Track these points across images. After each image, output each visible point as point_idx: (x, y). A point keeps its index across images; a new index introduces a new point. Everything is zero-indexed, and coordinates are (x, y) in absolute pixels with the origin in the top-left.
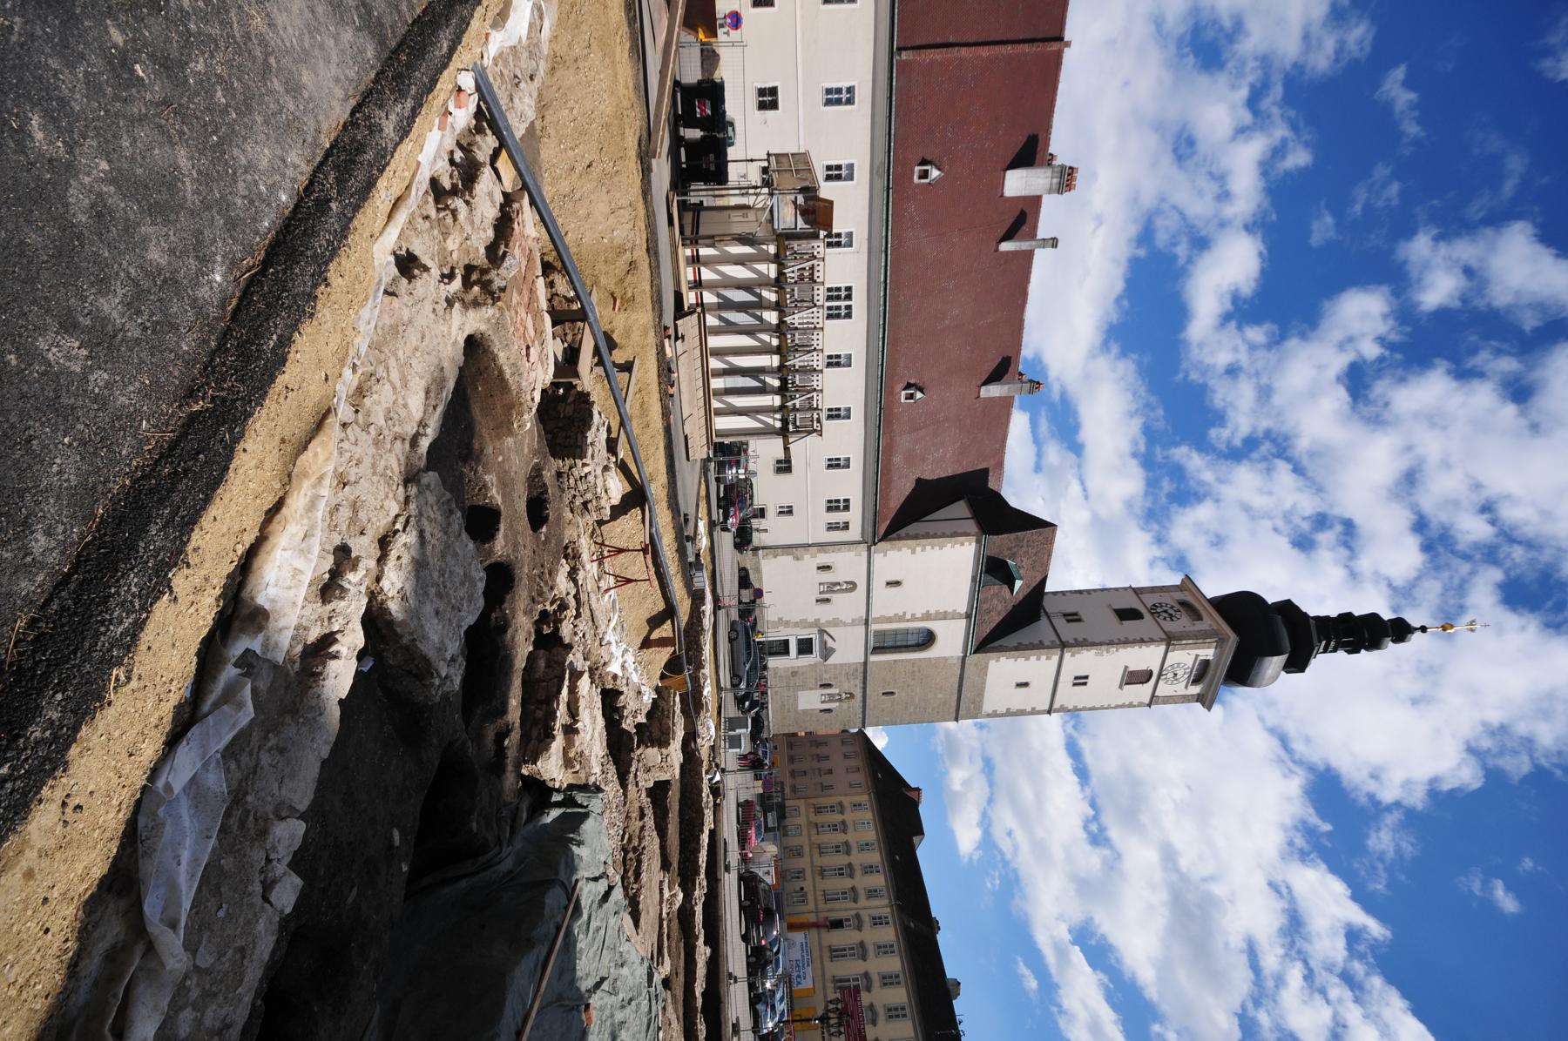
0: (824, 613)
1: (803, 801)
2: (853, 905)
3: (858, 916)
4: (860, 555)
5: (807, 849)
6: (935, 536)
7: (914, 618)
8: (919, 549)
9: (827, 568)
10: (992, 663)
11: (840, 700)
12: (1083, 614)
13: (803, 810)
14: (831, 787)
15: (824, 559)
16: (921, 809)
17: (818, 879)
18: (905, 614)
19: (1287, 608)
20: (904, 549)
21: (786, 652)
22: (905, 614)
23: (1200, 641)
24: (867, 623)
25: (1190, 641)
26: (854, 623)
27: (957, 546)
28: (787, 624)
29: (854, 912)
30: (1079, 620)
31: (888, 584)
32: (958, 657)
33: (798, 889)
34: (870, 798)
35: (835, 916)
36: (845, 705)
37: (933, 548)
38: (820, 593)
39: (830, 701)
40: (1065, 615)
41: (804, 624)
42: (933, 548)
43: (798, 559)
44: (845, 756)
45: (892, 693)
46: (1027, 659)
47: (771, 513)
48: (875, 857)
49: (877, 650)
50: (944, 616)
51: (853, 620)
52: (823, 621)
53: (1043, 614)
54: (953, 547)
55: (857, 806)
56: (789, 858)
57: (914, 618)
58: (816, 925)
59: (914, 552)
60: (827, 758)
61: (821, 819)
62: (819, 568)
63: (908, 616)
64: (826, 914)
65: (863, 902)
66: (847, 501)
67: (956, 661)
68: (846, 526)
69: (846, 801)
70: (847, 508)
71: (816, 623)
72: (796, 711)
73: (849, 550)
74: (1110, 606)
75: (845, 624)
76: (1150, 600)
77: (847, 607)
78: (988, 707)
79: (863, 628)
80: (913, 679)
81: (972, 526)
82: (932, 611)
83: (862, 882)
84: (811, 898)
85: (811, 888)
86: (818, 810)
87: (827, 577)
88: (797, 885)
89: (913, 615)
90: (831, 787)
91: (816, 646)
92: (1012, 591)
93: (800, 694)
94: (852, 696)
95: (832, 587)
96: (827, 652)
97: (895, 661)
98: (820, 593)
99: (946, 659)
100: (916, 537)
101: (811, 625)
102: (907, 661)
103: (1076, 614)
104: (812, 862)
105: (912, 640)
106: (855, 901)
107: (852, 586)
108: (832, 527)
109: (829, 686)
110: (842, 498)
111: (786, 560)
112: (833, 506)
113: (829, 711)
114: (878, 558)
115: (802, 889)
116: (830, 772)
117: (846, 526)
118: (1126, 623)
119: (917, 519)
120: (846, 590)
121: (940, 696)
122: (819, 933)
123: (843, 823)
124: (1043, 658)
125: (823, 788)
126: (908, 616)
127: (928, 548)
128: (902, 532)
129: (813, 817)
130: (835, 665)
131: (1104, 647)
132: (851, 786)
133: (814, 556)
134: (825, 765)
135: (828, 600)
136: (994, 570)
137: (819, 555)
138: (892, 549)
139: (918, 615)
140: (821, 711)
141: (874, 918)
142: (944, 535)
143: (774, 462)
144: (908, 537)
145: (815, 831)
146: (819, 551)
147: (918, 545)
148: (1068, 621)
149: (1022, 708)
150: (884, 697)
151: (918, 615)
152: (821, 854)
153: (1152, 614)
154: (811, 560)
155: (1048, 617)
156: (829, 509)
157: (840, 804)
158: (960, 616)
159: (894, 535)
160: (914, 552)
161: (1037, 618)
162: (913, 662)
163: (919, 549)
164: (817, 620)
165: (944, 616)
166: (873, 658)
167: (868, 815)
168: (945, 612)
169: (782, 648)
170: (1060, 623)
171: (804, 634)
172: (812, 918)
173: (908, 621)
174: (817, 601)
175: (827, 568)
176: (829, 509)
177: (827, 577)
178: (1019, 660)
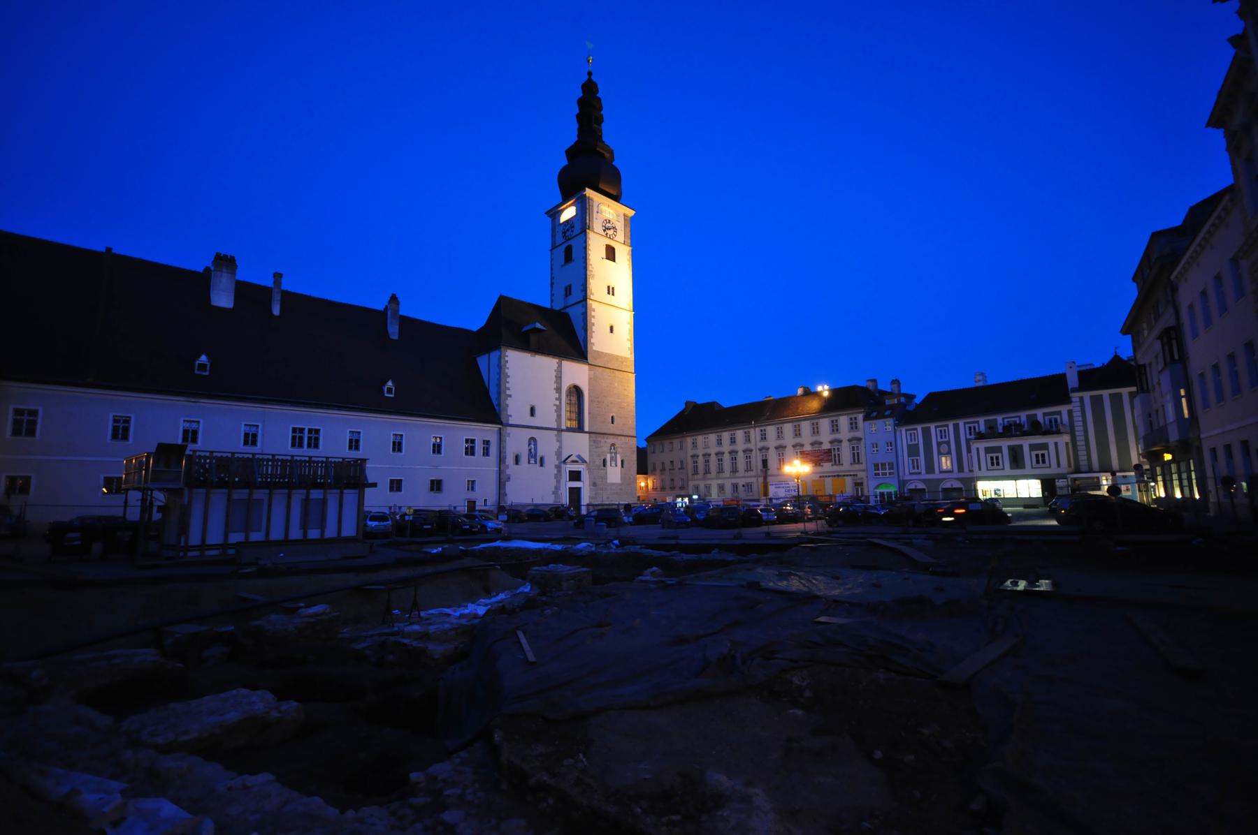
0: (551, 461)
1: (690, 483)
2: (754, 452)
3: (760, 450)
4: (509, 434)
5: (720, 481)
6: (499, 380)
7: (559, 399)
8: (508, 392)
9: (517, 460)
10: (594, 348)
11: (616, 453)
12: (567, 284)
13: (696, 483)
14: (682, 462)
15: (510, 460)
16: (700, 402)
17: (737, 474)
18: (555, 405)
19: (570, 153)
20: (507, 402)
21: (579, 489)
22: (555, 405)
23: (588, 211)
25: (588, 217)
26: (559, 440)
28: (557, 488)
29: (758, 452)
30: (570, 286)
32: (590, 370)
33: (743, 488)
34: (689, 436)
35: (760, 464)
36: (619, 450)
38: (536, 462)
39: (616, 461)
40: (566, 296)
41: (558, 476)
43: (509, 478)
44: (663, 451)
46: (593, 324)
47: (472, 496)
48: (726, 436)
51: (558, 441)
52: (557, 463)
53: (562, 311)
55: (695, 445)
56: (724, 493)
57: (559, 399)
58: (765, 478)
59: (510, 396)
60: (663, 463)
61: (701, 470)
63: (557, 403)
64: (759, 471)
65: (751, 446)
66: (467, 441)
67: (592, 372)
69: (691, 452)
70: (473, 441)
71: (558, 467)
72: (621, 484)
73: (505, 441)
74: (562, 266)
75: (560, 447)
76: (560, 239)
77: (547, 444)
79: (563, 433)
81: (494, 355)
82: (555, 386)
83: (740, 445)
84: (749, 480)
85: (743, 479)
86: (696, 472)
87: (524, 459)
88: (741, 489)
89: (557, 399)
90: (682, 462)
91: (575, 467)
92: (543, 330)
94: (613, 445)
95: (532, 455)
96: (581, 460)
97: (589, 413)
99: (590, 379)
100: (499, 393)
101: (559, 471)
103: (566, 288)
104: (729, 478)
105: (574, 399)
106: (751, 450)
107: (533, 440)
108: (486, 453)
109: (604, 461)
110: (465, 445)
111: (509, 487)
112: (470, 451)
113: (622, 461)
114: (511, 421)
115: (743, 486)
116: (672, 462)
117: (487, 443)
118: (573, 257)
119: (486, 392)
120: (535, 445)
122: (771, 476)
123: (704, 455)
124: (593, 314)
125: (682, 468)
126: (557, 403)
127: (507, 385)
128: (495, 402)
129: (700, 476)
130: (590, 456)
131: (588, 272)
132: (681, 448)
133: (508, 467)
134: (668, 466)
135: (542, 459)
136: (527, 343)
137: (507, 464)
138: (507, 411)
139: (557, 395)
140: (622, 467)
141: (762, 439)
142: (499, 373)
143: (432, 493)
144: (499, 399)
145: (709, 475)
146: (505, 463)
147: (505, 392)
148: (570, 294)
151: (557, 395)
152: (723, 472)
153: (569, 239)
154: (511, 469)
155: (567, 307)
156: (473, 454)
157: (692, 456)
158: (560, 366)
159: (496, 408)
160: (510, 396)
161: (567, 315)
162: (591, 402)
163: (508, 392)
164: (556, 467)
165: (559, 378)
166: (586, 429)
167: (700, 439)
168: (556, 377)
169: (575, 493)
170: (571, 300)
171: (566, 476)
172: (761, 480)
173: (560, 403)
175: (517, 460)
176: (473, 454)
177: (524, 459)
178: (593, 330)
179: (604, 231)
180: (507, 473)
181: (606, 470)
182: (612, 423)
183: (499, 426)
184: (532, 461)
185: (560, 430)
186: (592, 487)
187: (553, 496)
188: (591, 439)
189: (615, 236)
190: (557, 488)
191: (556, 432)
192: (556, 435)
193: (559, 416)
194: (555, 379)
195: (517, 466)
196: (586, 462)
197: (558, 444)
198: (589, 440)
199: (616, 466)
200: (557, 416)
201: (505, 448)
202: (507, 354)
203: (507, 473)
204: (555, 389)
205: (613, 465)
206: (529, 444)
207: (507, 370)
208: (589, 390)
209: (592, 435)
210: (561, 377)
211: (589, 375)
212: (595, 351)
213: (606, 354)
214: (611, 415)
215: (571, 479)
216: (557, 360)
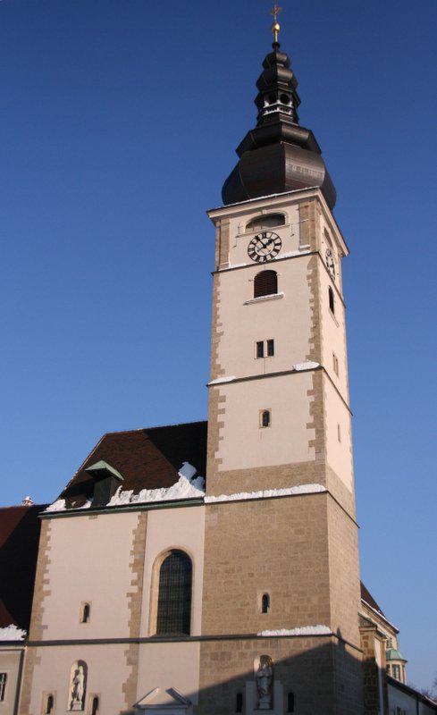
7: (139, 582)
8: (46, 587)
18: (128, 595)
20: (43, 605)
22: (128, 595)
24: (136, 641)
26: (133, 662)
27: (49, 544)
31: (85, 621)
37: (47, 571)
42: (47, 571)
49: (186, 629)
51: (130, 662)
54: (49, 549)
59: (48, 593)
63: (135, 589)
67: (215, 516)
78: (311, 455)
79: (142, 646)
80: (240, 570)
82: (131, 560)
89: (134, 583)
97: (205, 598)
99: (209, 530)
102: (206, 579)
114: (46, 637)
126: (135, 589)
127: (46, 577)
139: (135, 576)
151: (135, 576)
160: (48, 593)
162: (209, 574)
166: (197, 629)
168: (135, 542)
173: (141, 589)
178: (221, 435)
179: (251, 256)
182: (265, 611)
185: (136, 641)
188: (208, 651)
189: (277, 251)
191: (126, 646)
192: (127, 652)
197: (131, 667)
200: (133, 613)
202: (50, 526)
204: (130, 565)
207: (47, 553)
208: (206, 551)
212: (222, 474)
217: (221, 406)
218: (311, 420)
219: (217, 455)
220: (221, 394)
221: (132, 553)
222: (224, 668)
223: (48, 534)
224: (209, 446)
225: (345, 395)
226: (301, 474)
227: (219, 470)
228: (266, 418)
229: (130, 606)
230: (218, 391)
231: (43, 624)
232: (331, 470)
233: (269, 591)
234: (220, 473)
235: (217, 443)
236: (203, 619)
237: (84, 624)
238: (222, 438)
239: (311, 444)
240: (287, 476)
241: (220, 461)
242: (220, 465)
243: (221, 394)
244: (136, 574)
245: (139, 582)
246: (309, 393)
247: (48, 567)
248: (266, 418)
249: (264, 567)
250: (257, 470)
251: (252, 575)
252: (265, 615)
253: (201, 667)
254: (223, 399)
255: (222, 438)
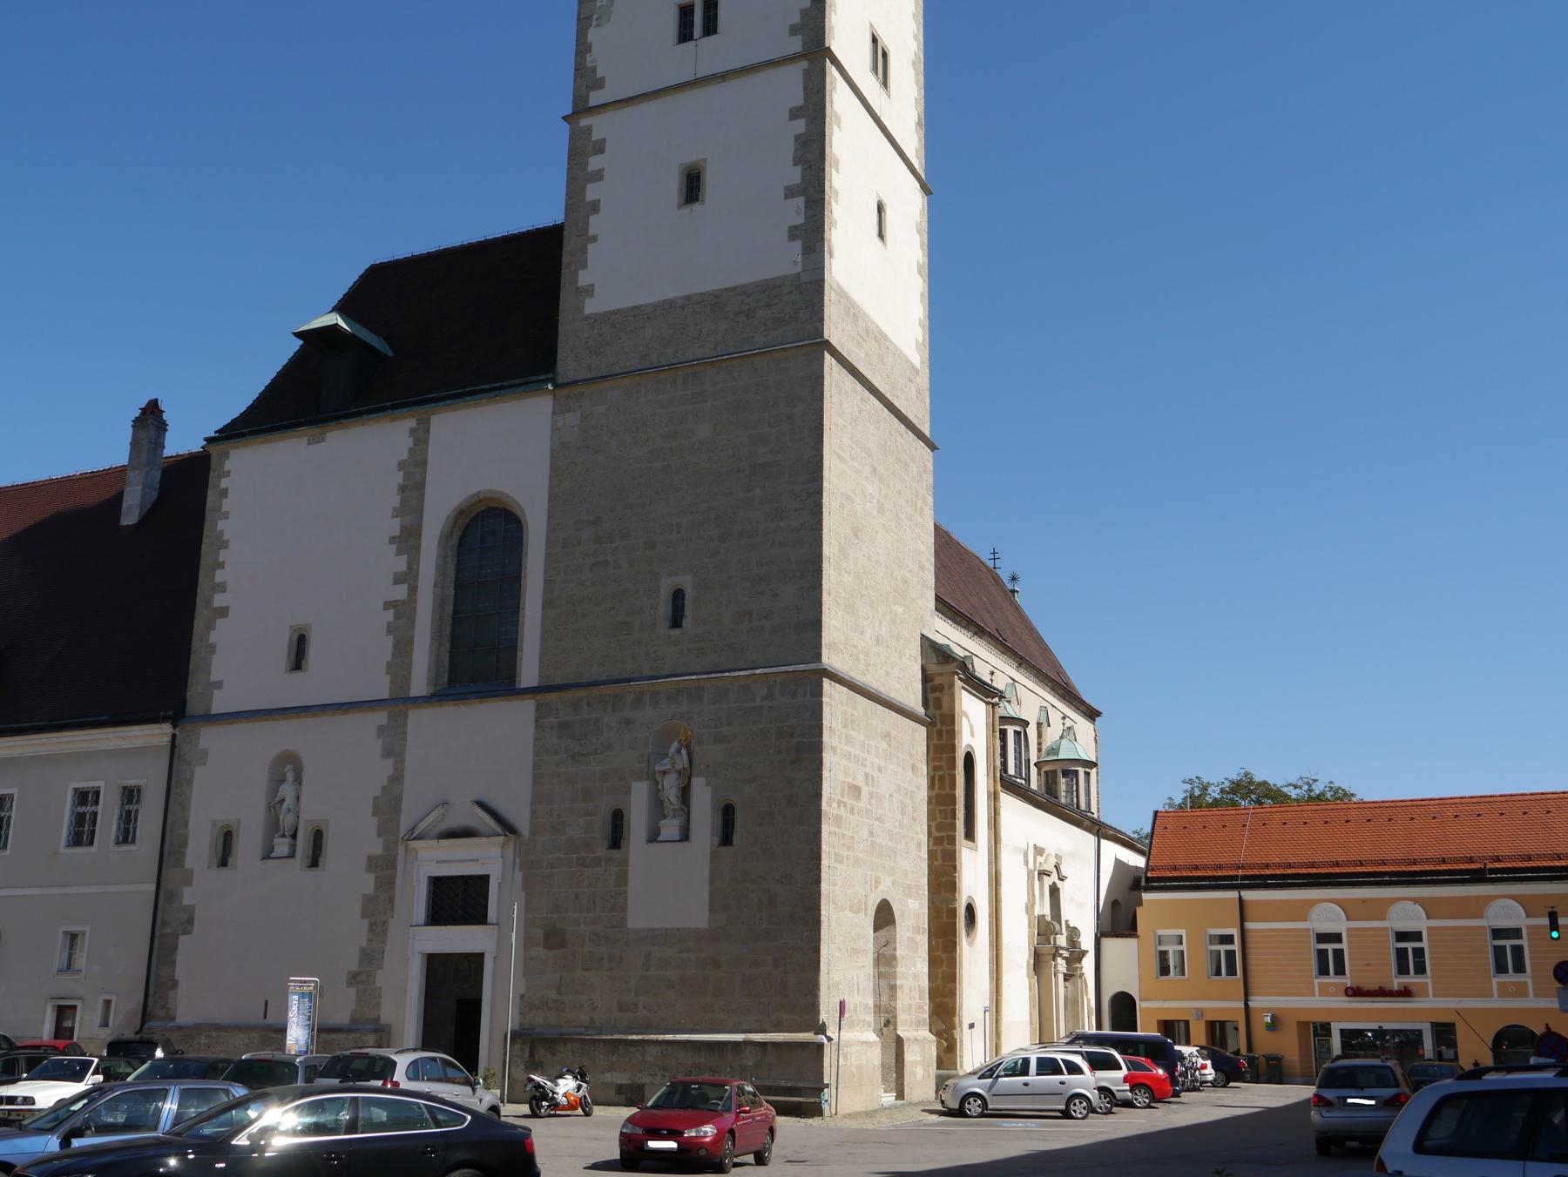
4: (205, 752)
7: (408, 578)
18: (388, 605)
20: (214, 637)
21: (473, 962)
22: (388, 605)
26: (394, 749)
27: (227, 505)
37: (221, 565)
38: (292, 855)
41: (378, 909)
42: (221, 565)
43: (190, 921)
45: (678, 596)
50: (413, 488)
51: (388, 752)
52: (376, 847)
59: (223, 612)
62: (224, 863)
63: (401, 592)
67: (573, 418)
68: (131, 795)
71: (384, 868)
73: (190, 782)
75: (397, 778)
82: (394, 527)
89: (398, 579)
91: (458, 859)
93: (636, 920)
97: (548, 604)
98: (292, 855)
109: (618, 820)
114: (220, 703)
121: (704, 432)
126: (401, 592)
127: (220, 576)
130: (536, 800)
133: (188, 878)
137: (189, 864)
139: (401, 564)
140: (726, 839)
146: (180, 862)
147: (209, 603)
149: (788, 149)
150: (687, 622)
151: (401, 564)
158: (421, 440)
160: (223, 612)
163: (219, 601)
164: (373, 863)
165: (413, 488)
166: (528, 674)
168: (402, 489)
173: (413, 590)
174: (314, 863)
180: (186, 901)
181: (625, 862)
182: (676, 622)
183: (166, 729)
184: (282, 846)
185: (399, 702)
186: (539, 951)
187: (353, 991)
190: (371, 958)
191: (381, 717)
192: (381, 729)
193: (403, 648)
194: (396, 501)
195: (223, 872)
196: (508, 828)
197: (388, 766)
198: (539, 726)
199: (685, 836)
200: (395, 646)
201: (185, 807)
202: (228, 465)
203: (186, 901)
204: (392, 540)
205: (670, 828)
206: (277, 781)
207: (221, 525)
208: (552, 498)
209: (553, 697)
210: (421, 486)
211: (555, 430)
213: (654, 306)
214: (666, 586)
215: (438, 915)
216: (411, 423)
217: (594, 163)
218: (795, 175)
219: (584, 278)
220: (596, 136)
221: (398, 513)
222: (584, 755)
223: (224, 483)
224: (566, 258)
225: (912, 143)
226: (768, 306)
227: (587, 312)
228: (692, 186)
229: (391, 629)
230: (589, 129)
231: (213, 679)
232: (843, 294)
233: (686, 582)
234: (587, 318)
235: (584, 250)
236: (544, 652)
237: (298, 675)
238: (594, 239)
239: (794, 233)
240: (737, 314)
241: (589, 291)
242: (588, 301)
243: (596, 136)
244: (404, 558)
245: (408, 578)
246: (795, 114)
247: (223, 555)
248: (692, 186)
249: (679, 525)
250: (668, 306)
251: (651, 545)
252: (677, 631)
253: (536, 754)
254: (600, 148)
255: (594, 239)
